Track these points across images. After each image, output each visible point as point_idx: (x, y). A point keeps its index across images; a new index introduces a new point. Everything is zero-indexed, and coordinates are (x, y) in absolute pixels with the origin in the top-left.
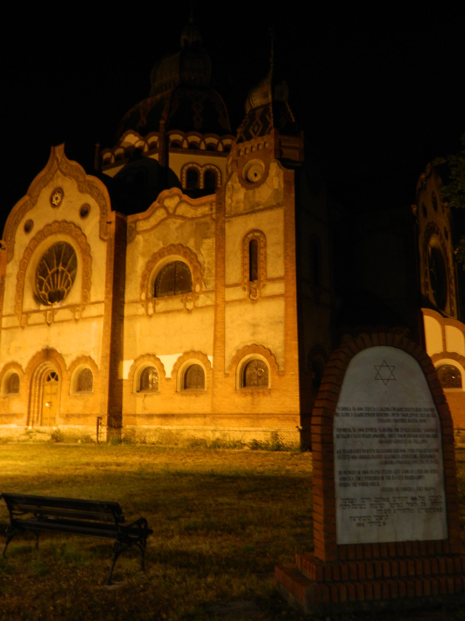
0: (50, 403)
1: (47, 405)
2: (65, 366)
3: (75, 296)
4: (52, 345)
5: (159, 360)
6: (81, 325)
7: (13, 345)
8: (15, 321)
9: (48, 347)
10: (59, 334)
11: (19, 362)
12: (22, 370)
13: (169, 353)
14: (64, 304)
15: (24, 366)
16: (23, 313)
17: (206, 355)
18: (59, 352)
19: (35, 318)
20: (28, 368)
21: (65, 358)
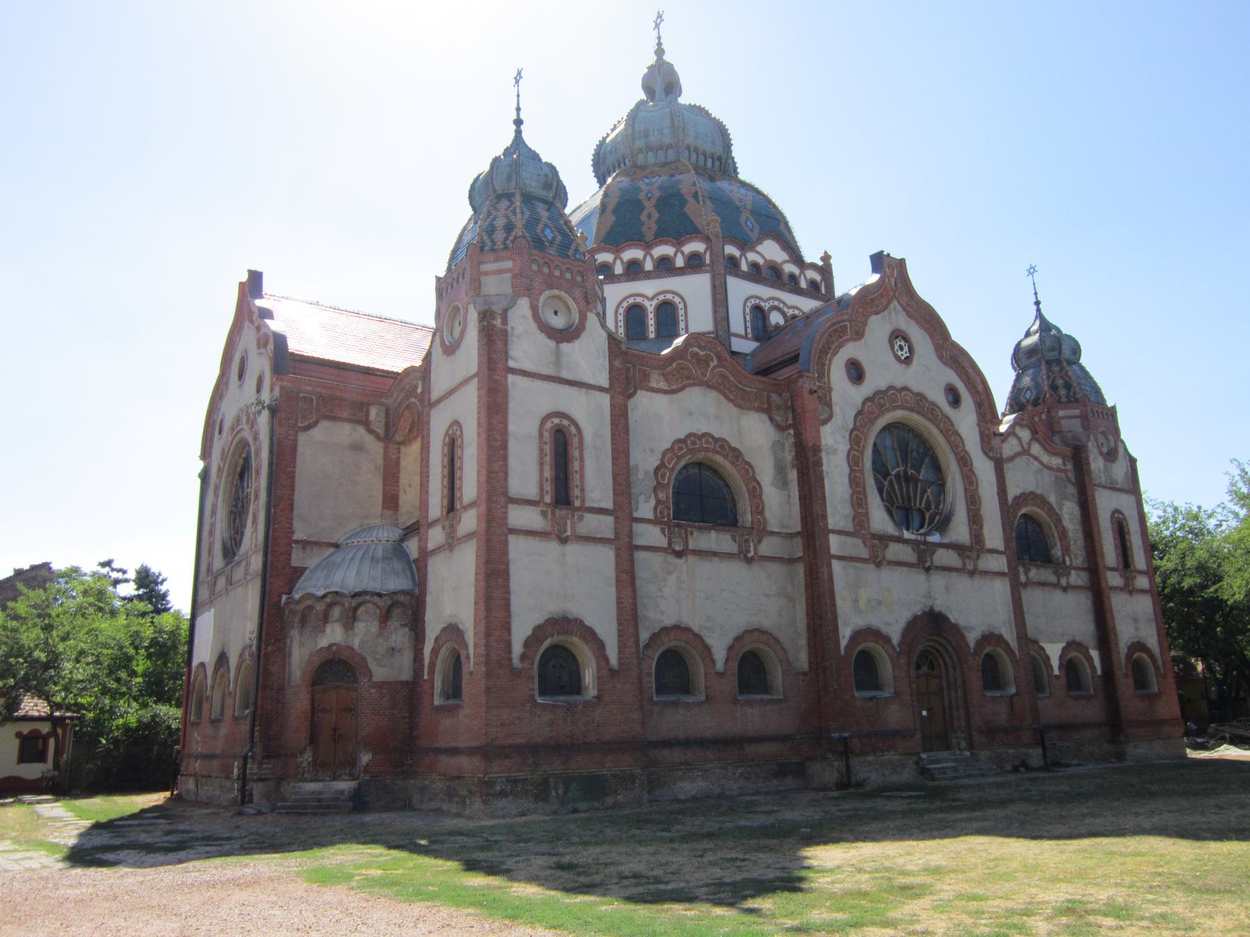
0: (929, 710)
1: (924, 713)
2: (967, 645)
3: (960, 531)
4: (939, 606)
5: (1043, 649)
6: (978, 581)
7: (864, 594)
8: (856, 547)
9: (932, 608)
10: (947, 589)
11: (884, 630)
12: (893, 647)
13: (1052, 641)
14: (946, 541)
15: (896, 638)
16: (874, 536)
17: (1087, 649)
18: (953, 621)
19: (895, 551)
20: (900, 644)
21: (967, 634)
